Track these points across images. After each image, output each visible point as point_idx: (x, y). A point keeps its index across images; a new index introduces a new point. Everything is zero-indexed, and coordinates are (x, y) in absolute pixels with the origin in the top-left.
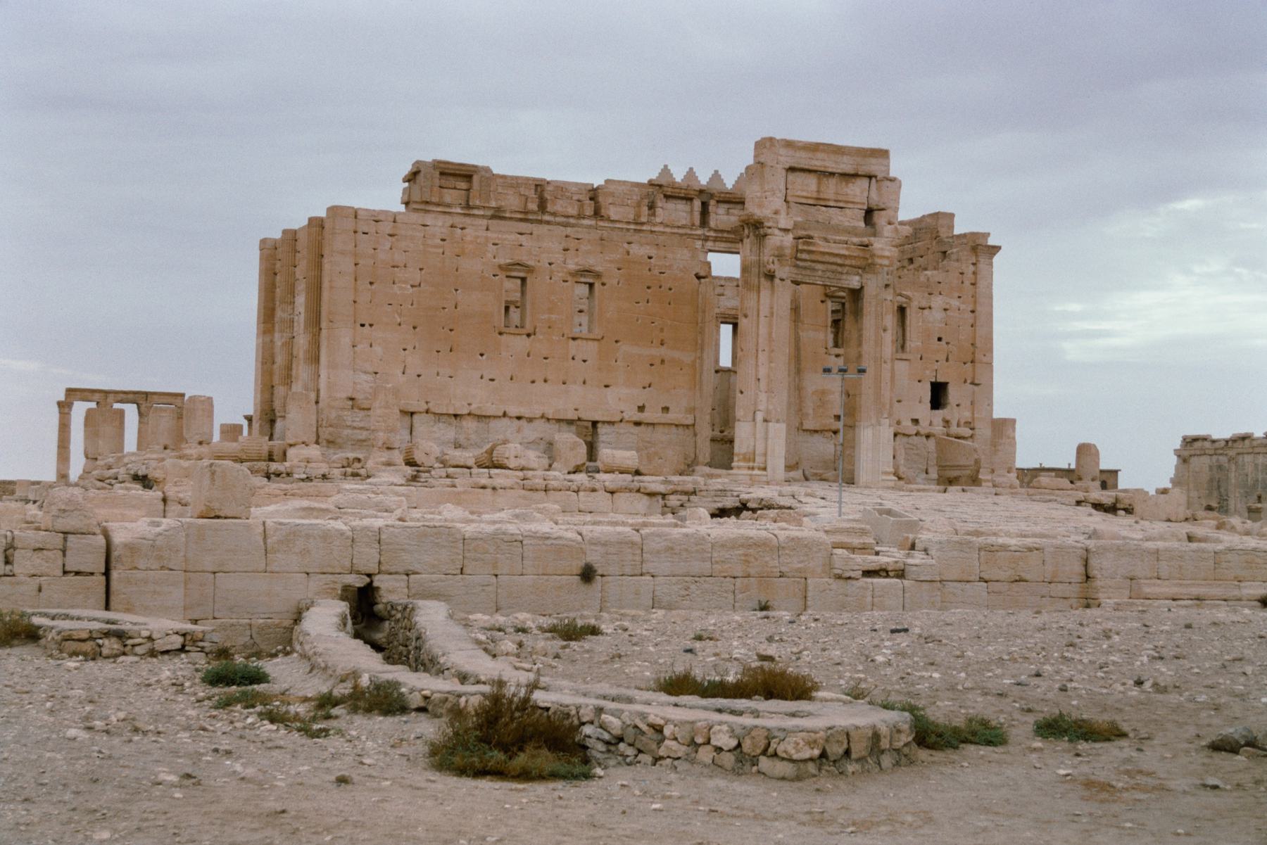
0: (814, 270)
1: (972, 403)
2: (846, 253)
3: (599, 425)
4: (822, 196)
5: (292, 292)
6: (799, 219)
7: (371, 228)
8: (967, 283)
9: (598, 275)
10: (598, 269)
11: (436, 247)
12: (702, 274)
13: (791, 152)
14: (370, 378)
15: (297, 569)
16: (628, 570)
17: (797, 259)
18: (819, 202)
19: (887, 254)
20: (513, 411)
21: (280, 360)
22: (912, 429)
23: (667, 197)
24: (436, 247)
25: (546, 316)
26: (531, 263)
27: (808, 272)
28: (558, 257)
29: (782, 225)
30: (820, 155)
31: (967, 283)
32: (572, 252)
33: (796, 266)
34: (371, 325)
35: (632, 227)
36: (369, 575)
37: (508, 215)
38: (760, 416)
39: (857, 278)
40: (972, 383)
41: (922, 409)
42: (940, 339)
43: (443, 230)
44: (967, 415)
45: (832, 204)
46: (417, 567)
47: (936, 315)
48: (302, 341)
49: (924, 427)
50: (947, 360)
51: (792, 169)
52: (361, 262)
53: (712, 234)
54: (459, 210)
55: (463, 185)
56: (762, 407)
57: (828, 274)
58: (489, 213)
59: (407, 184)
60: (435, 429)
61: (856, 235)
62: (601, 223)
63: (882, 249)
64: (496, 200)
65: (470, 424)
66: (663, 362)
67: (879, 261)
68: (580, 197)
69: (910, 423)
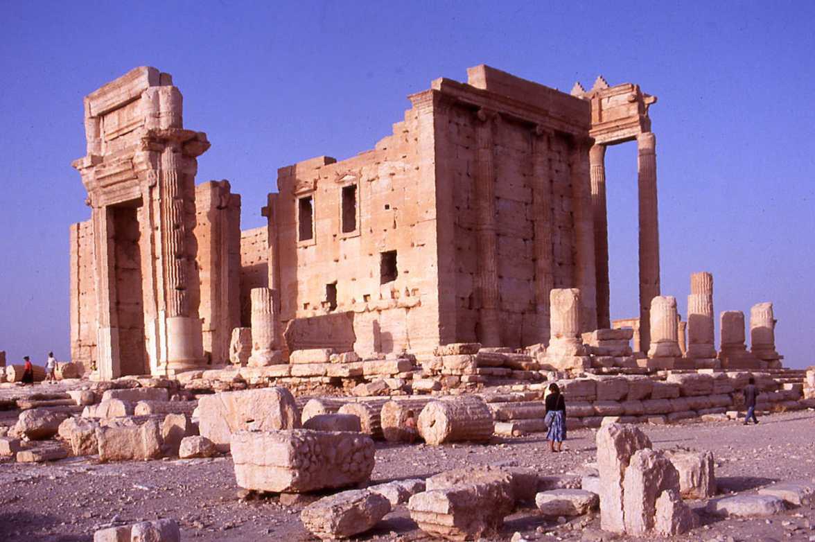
2: (118, 170)
30: (110, 95)
42: (387, 207)
45: (126, 131)
47: (384, 182)
57: (122, 192)
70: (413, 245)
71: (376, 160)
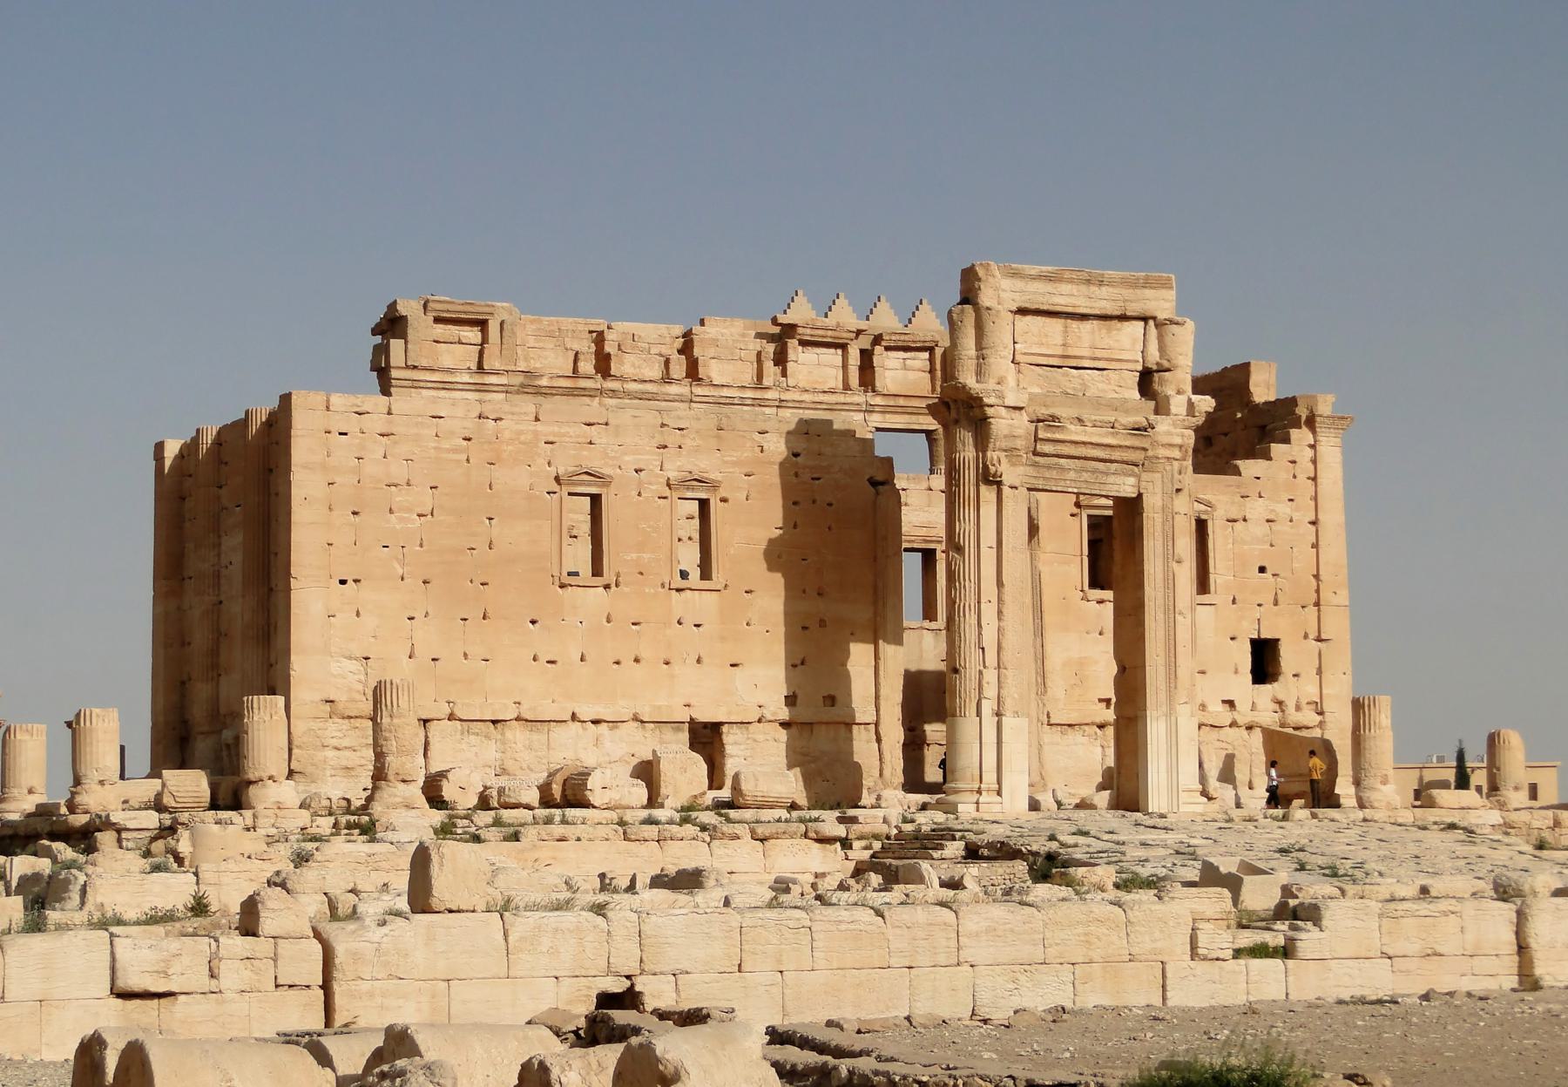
0: (1062, 469)
1: (1319, 672)
3: (725, 729)
4: (1070, 352)
5: (216, 529)
6: (1037, 390)
7: (352, 424)
8: (1302, 477)
9: (714, 486)
10: (712, 476)
11: (455, 451)
12: (879, 478)
13: (1019, 284)
14: (355, 666)
15: (543, 973)
16: (942, 960)
17: (1035, 453)
18: (1066, 363)
19: (1178, 441)
20: (586, 713)
21: (200, 638)
22: (1225, 716)
23: (804, 343)
24: (455, 451)
25: (634, 556)
26: (606, 471)
27: (1054, 474)
28: (650, 459)
29: (1010, 401)
30: (1065, 288)
31: (1302, 477)
32: (671, 451)
33: (1035, 465)
34: (356, 581)
35: (749, 394)
36: (628, 977)
37: (544, 382)
38: (988, 707)
39: (1132, 480)
40: (1319, 639)
41: (1241, 685)
42: (1262, 570)
43: (468, 424)
44: (1311, 691)
46: (685, 966)
47: (1257, 529)
48: (239, 610)
49: (1244, 714)
50: (1276, 603)
51: (1022, 311)
52: (337, 479)
53: (878, 400)
54: (466, 378)
55: (473, 334)
56: (990, 691)
57: (1085, 476)
58: (518, 380)
59: (378, 339)
60: (464, 746)
61: (1127, 412)
62: (698, 390)
63: (1169, 433)
64: (526, 359)
65: (516, 734)
66: (822, 623)
67: (1162, 452)
68: (665, 350)
69: (1221, 708)
70: (1306, 636)
71: (1244, 492)
